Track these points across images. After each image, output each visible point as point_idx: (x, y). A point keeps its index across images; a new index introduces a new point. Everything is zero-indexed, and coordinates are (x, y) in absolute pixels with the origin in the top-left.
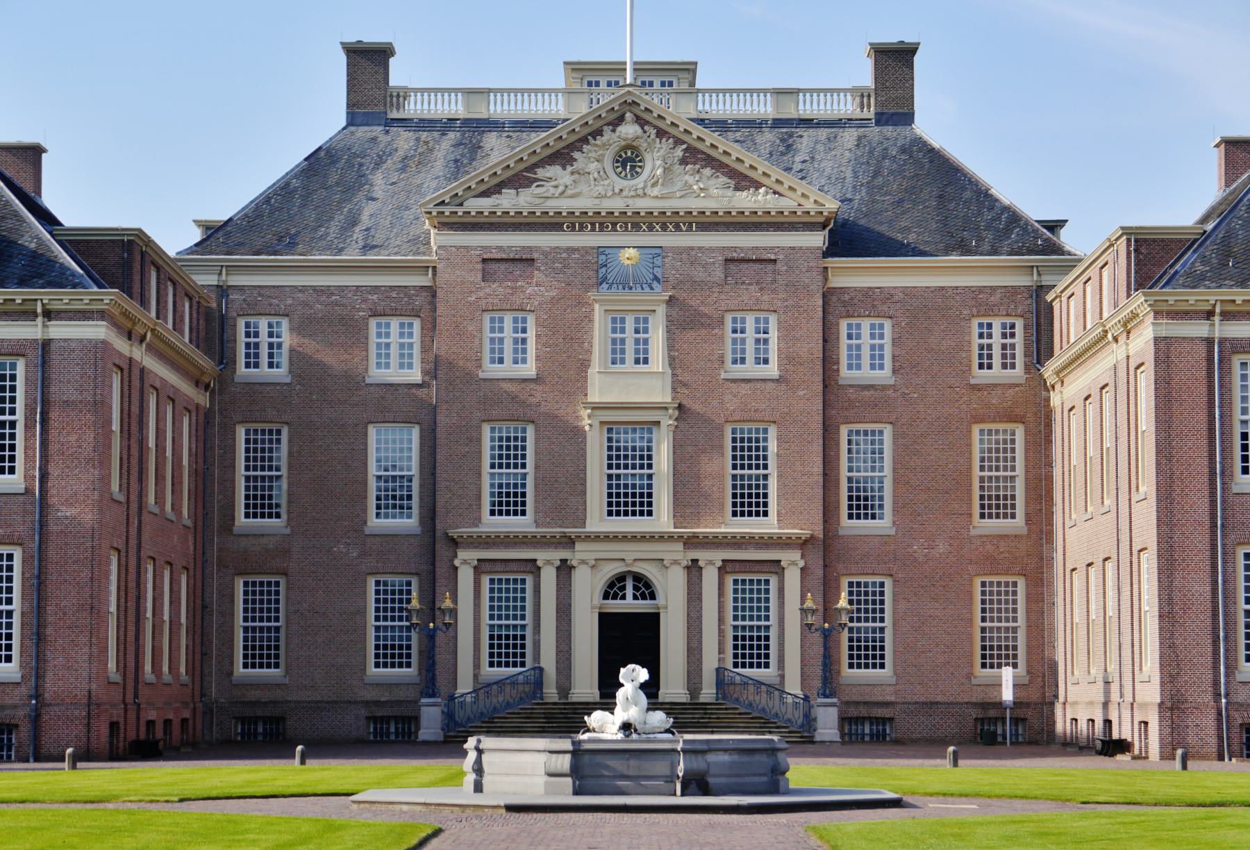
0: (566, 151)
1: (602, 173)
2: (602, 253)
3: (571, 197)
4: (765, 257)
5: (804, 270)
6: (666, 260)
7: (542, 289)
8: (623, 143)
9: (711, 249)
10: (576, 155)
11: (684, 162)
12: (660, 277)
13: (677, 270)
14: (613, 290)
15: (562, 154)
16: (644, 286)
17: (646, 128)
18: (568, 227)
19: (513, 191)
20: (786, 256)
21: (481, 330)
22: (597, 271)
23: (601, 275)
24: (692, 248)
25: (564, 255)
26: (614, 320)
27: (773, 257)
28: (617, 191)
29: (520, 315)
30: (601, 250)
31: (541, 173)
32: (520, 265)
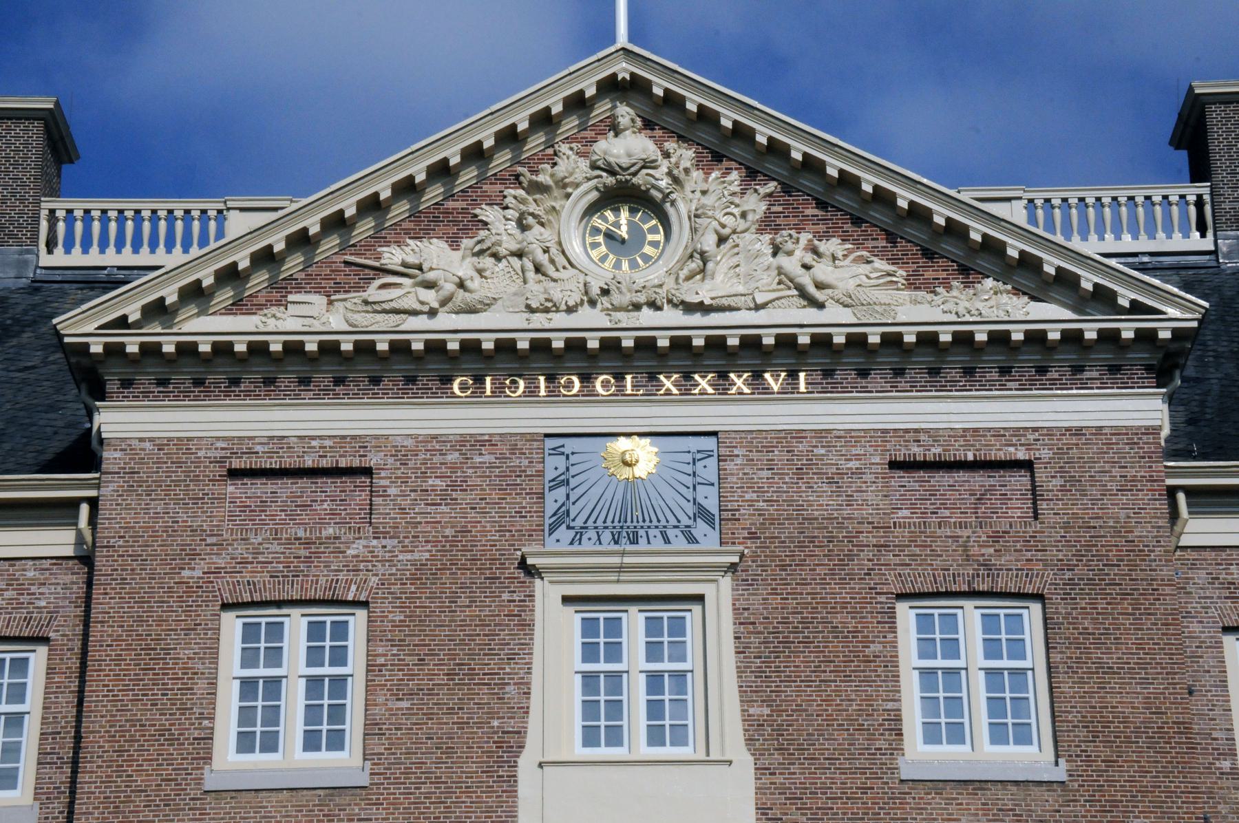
0: (460, 205)
1: (554, 251)
2: (556, 451)
3: (471, 310)
4: (1001, 456)
5: (1113, 486)
6: (729, 466)
7: (389, 543)
8: (610, 180)
9: (850, 437)
10: (489, 214)
11: (768, 224)
12: (715, 511)
13: (760, 491)
14: (587, 546)
15: (447, 212)
16: (671, 533)
17: (667, 145)
18: (463, 388)
19: (319, 300)
20: (1060, 453)
21: (212, 653)
22: (542, 496)
23: (550, 507)
24: (799, 435)
25: (453, 457)
26: (589, 627)
27: (1021, 455)
28: (595, 291)
29: (328, 615)
30: (551, 443)
31: (393, 256)
32: (330, 485)
